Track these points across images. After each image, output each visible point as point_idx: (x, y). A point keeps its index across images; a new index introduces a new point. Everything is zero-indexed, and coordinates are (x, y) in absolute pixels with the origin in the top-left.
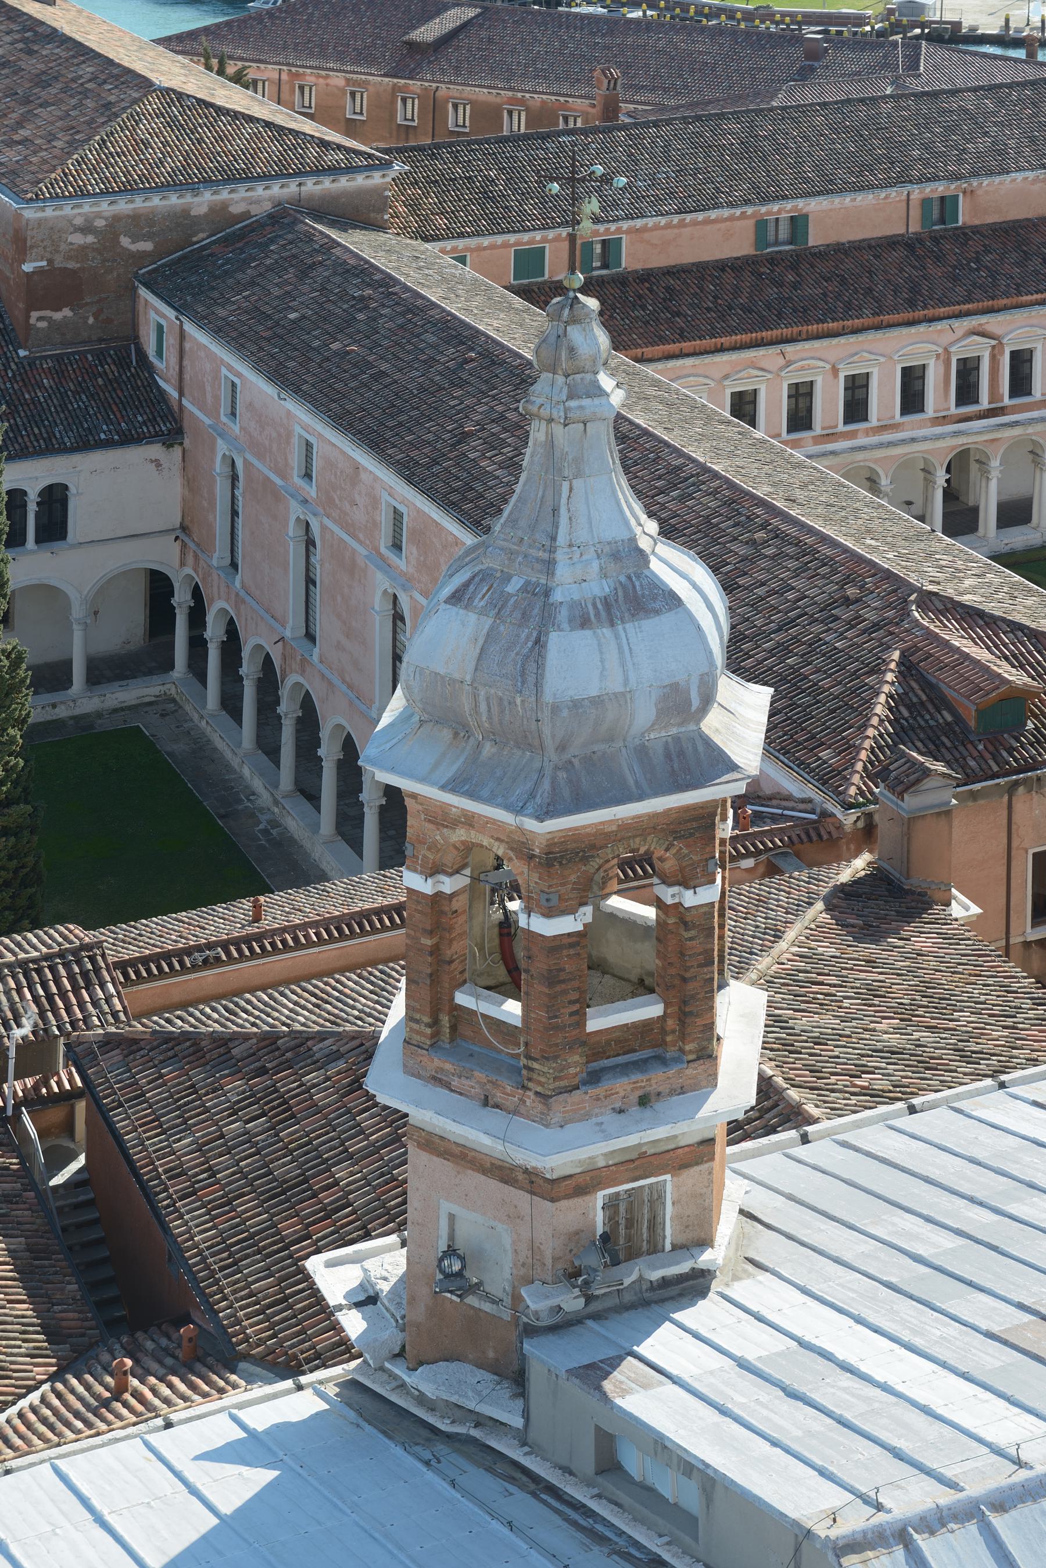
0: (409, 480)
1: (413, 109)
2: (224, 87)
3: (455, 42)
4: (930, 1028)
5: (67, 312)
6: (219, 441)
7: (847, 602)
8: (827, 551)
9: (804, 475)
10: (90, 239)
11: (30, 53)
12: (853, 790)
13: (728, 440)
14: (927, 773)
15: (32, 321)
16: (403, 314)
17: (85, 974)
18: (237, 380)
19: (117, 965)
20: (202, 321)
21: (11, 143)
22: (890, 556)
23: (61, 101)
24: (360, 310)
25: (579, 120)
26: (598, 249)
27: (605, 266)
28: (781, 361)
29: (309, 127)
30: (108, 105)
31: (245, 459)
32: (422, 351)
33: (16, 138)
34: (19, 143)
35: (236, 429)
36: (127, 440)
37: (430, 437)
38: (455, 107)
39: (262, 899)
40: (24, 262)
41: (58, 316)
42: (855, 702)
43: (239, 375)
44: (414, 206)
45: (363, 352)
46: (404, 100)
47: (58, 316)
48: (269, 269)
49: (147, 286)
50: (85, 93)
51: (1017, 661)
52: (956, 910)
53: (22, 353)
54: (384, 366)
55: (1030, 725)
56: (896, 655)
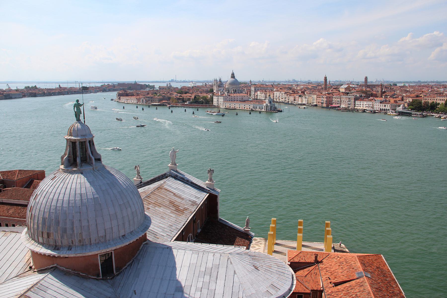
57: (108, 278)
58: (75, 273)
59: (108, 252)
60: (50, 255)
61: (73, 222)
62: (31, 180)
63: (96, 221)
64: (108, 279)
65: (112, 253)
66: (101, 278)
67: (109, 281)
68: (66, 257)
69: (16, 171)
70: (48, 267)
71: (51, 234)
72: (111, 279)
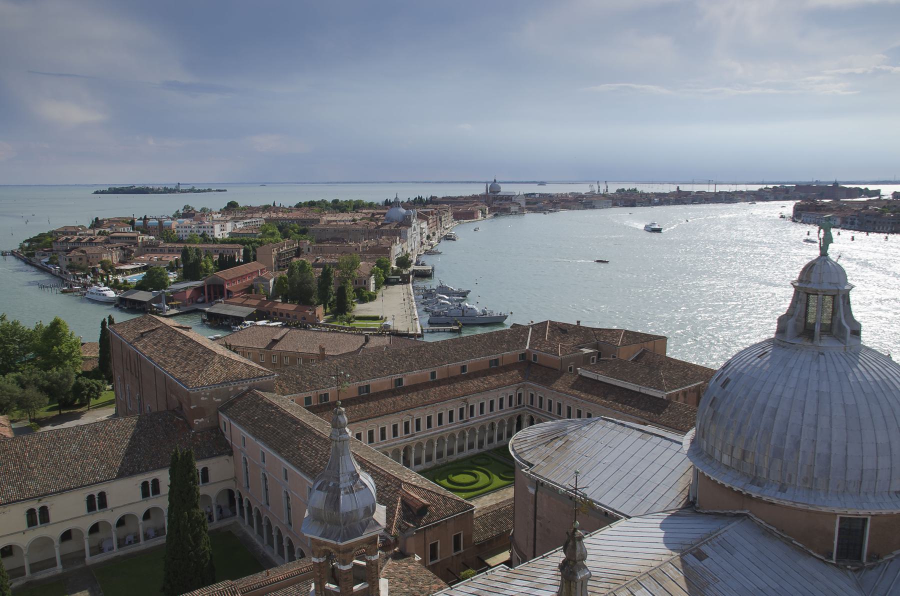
0: (288, 461)
1: (276, 358)
2: (234, 354)
3: (284, 339)
4: (414, 587)
5: (202, 419)
6: (242, 454)
7: (387, 486)
8: (382, 473)
9: (376, 454)
10: (206, 399)
11: (185, 345)
12: (393, 533)
13: (358, 446)
14: (409, 526)
15: (195, 422)
16: (282, 416)
17: (233, 592)
18: (245, 436)
19: (240, 589)
20: (234, 420)
21: (184, 372)
22: (396, 473)
23: (195, 360)
24: (272, 416)
25: (315, 361)
26: (323, 396)
27: (325, 401)
28: (366, 425)
29: (254, 364)
30: (206, 360)
31: (249, 459)
32: (287, 426)
33: (185, 370)
34: (186, 372)
35: (246, 449)
36: (221, 454)
37: (291, 449)
38: (285, 358)
39: (269, 571)
40: (191, 406)
41: (200, 421)
42: (391, 511)
43: (245, 435)
44: (281, 386)
45: (274, 427)
46: (273, 356)
47: (200, 421)
48: (249, 405)
49: (221, 411)
50: (200, 357)
51: (425, 498)
52: (416, 559)
53: (193, 431)
54: (279, 431)
55: (428, 513)
56: (400, 498)
57: (849, 567)
58: (782, 537)
59: (860, 515)
60: (741, 490)
61: (799, 442)
62: (642, 349)
63: (846, 449)
64: (848, 569)
65: (865, 520)
66: (835, 562)
67: (850, 573)
68: (773, 503)
69: (618, 331)
70: (730, 511)
71: (751, 453)
72: (855, 571)
